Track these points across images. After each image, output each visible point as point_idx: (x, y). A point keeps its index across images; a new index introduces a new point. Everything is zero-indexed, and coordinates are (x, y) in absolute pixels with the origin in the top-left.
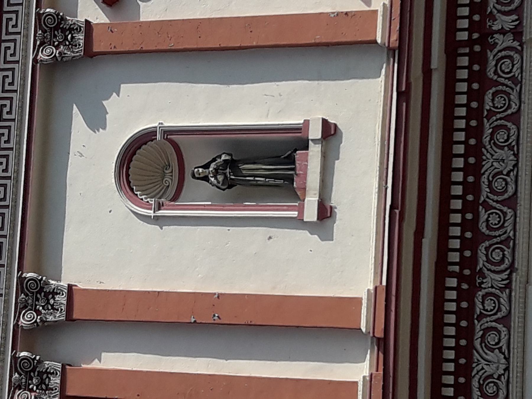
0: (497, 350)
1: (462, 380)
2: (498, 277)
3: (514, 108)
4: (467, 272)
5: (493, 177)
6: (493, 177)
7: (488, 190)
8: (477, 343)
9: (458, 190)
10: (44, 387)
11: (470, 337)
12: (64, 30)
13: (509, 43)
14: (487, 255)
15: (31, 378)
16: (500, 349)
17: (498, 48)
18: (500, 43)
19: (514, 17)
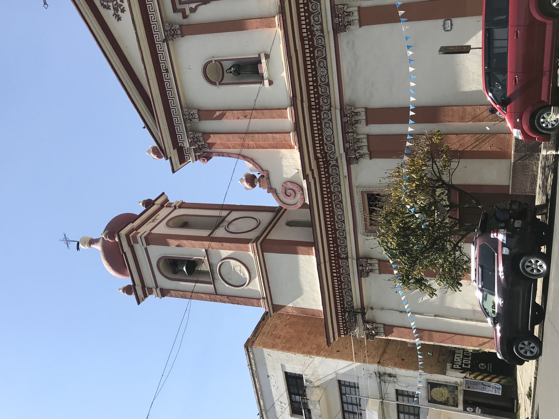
0: (329, 128)
1: (320, 137)
2: (326, 107)
3: (324, 55)
4: (317, 107)
5: (321, 77)
6: (321, 77)
7: (320, 81)
8: (323, 127)
9: (311, 83)
10: (199, 141)
11: (321, 125)
12: (173, 30)
13: (320, 34)
14: (323, 101)
15: (194, 139)
16: (330, 128)
17: (317, 36)
18: (317, 34)
19: (320, 26)
